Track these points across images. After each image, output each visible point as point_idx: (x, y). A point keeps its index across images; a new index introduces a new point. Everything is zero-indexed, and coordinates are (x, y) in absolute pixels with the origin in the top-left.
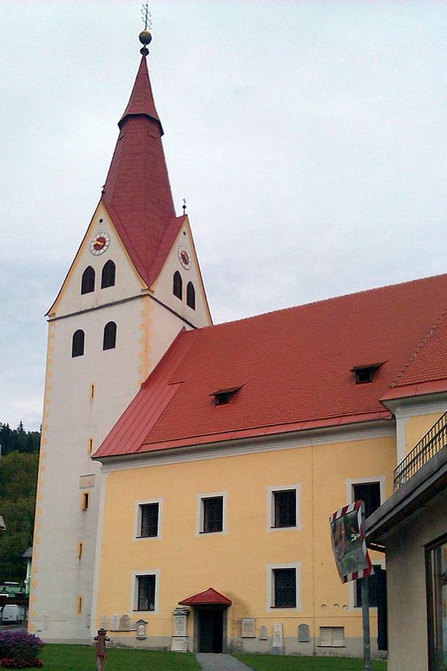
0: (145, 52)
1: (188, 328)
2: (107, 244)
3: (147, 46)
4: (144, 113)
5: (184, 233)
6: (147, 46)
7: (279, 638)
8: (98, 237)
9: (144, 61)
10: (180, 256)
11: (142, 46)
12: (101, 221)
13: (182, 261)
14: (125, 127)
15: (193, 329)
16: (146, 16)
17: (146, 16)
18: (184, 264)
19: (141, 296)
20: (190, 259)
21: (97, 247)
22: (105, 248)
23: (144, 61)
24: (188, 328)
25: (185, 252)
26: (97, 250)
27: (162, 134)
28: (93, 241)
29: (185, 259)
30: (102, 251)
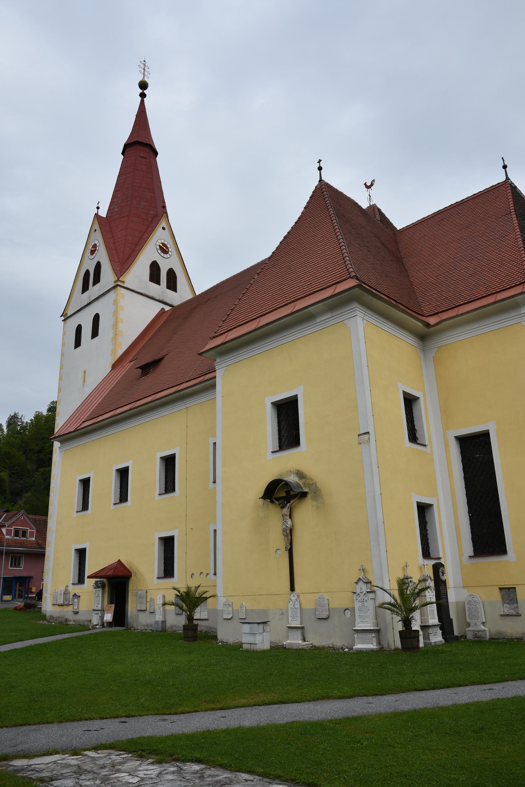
0: (143, 96)
1: (167, 308)
2: (97, 248)
3: (145, 91)
4: (135, 140)
5: (164, 228)
6: (145, 91)
7: (160, 611)
8: (93, 244)
9: (142, 103)
10: (158, 247)
11: (141, 91)
12: (95, 230)
13: (160, 251)
14: (125, 154)
15: (171, 308)
16: (144, 69)
17: (144, 69)
18: (162, 254)
19: (114, 287)
20: (170, 249)
21: (92, 252)
22: (96, 252)
23: (142, 103)
24: (167, 308)
25: (163, 244)
26: (92, 255)
27: (156, 153)
28: (90, 247)
29: (164, 249)
30: (94, 255)
